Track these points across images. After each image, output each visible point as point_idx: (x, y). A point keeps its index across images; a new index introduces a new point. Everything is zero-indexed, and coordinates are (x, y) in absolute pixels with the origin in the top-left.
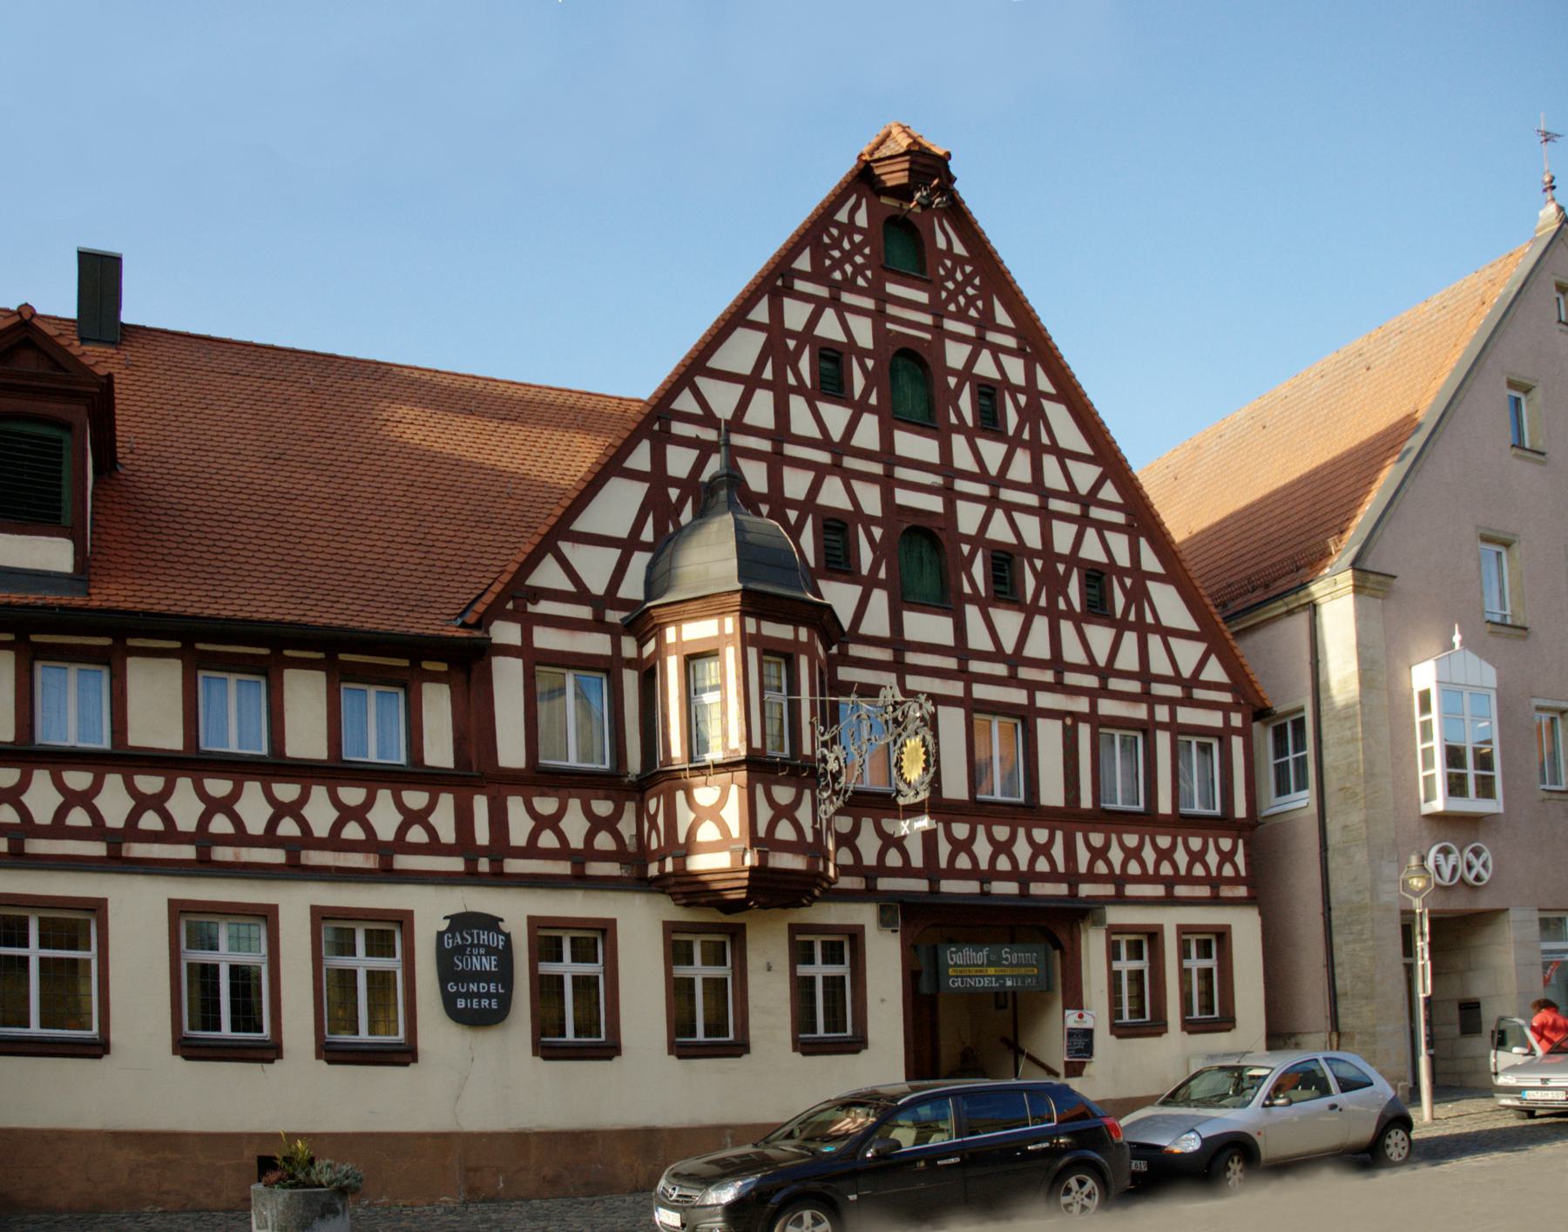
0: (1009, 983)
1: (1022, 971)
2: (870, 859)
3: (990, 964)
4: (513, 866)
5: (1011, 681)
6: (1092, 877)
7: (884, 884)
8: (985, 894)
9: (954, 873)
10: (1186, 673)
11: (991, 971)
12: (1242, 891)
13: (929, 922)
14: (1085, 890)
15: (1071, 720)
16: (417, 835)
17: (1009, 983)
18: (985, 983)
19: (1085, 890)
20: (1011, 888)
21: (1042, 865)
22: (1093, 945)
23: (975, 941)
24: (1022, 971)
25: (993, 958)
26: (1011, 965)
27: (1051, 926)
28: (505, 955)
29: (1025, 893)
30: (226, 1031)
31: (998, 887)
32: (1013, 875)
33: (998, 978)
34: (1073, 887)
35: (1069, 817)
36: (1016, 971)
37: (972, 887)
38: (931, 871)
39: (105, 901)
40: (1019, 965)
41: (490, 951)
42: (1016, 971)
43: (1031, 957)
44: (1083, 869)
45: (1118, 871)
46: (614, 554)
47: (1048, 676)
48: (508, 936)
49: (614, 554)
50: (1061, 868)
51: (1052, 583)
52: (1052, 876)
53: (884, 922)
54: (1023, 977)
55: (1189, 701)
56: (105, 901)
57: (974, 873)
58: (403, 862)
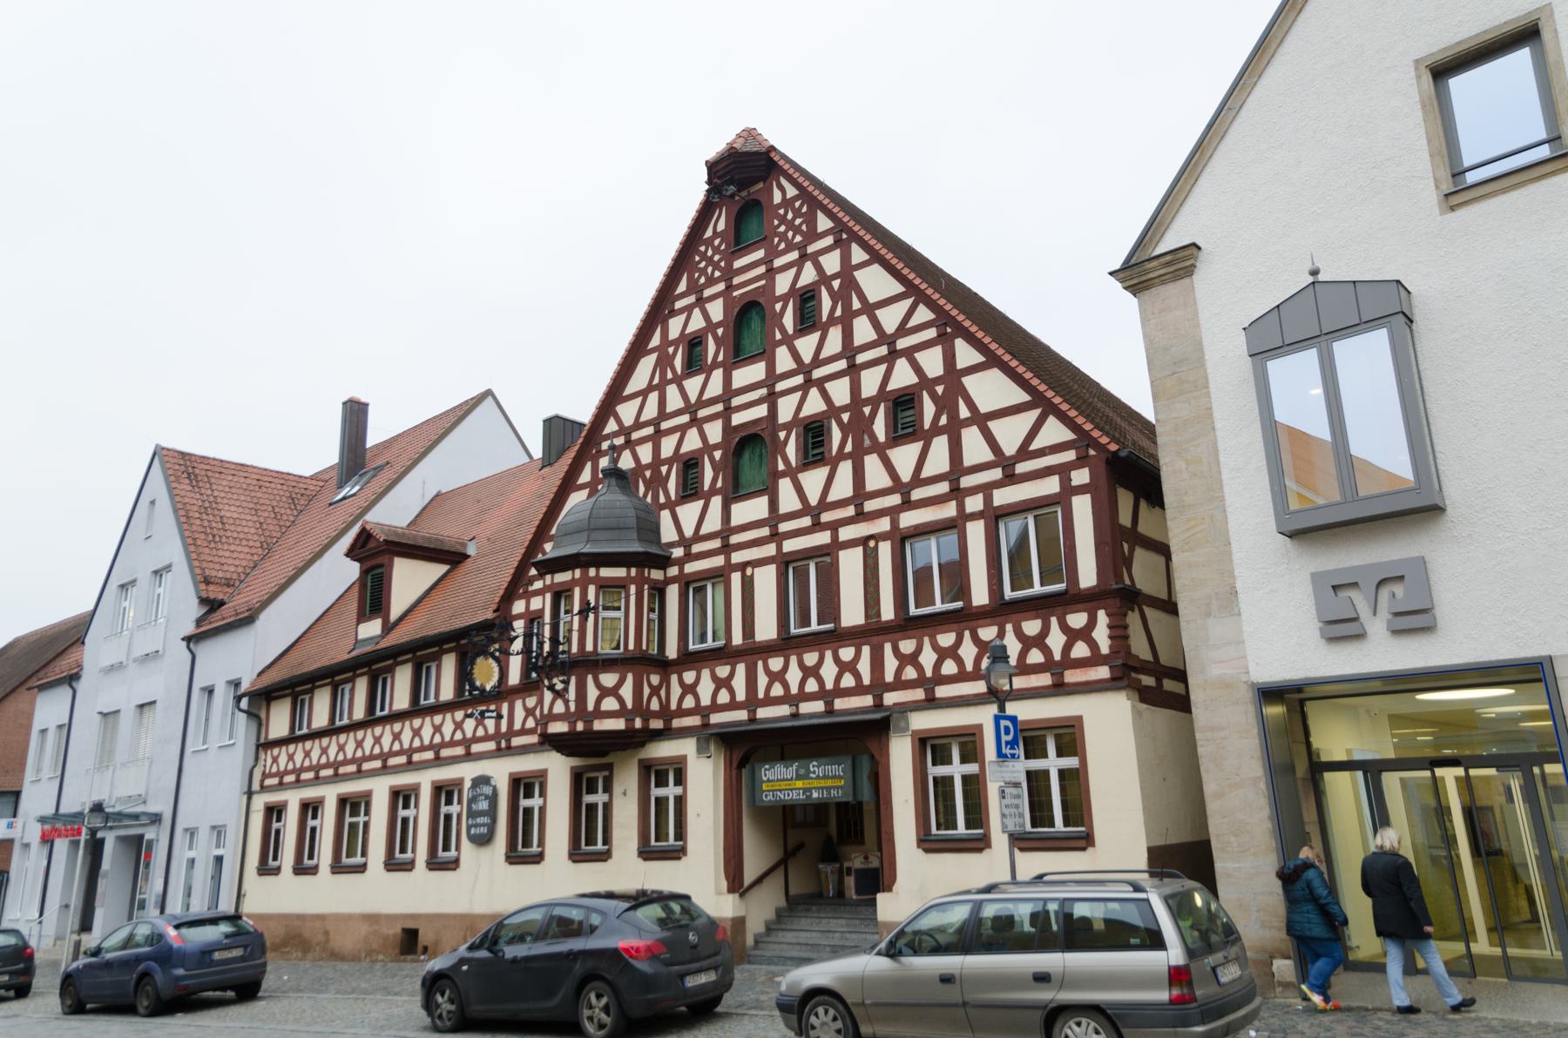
0: (815, 795)
1: (829, 783)
2: (706, 701)
3: (799, 777)
4: (516, 741)
5: (817, 526)
6: (899, 684)
7: (715, 718)
8: (795, 716)
9: (769, 701)
10: (814, 500)
11: (799, 784)
12: (1103, 672)
13: (746, 748)
14: (890, 698)
15: (867, 544)
16: (949, 668)
17: (815, 795)
18: (794, 796)
19: (890, 698)
20: (818, 706)
21: (848, 681)
22: (901, 755)
23: (784, 757)
24: (829, 783)
25: (802, 772)
26: (818, 777)
27: (860, 739)
28: (493, 799)
29: (830, 711)
30: (962, 829)
31: (806, 708)
32: (822, 694)
33: (805, 790)
34: (753, 712)
35: (873, 632)
36: (823, 783)
37: (784, 710)
38: (752, 702)
39: (1079, 719)
40: (825, 777)
41: (487, 797)
42: (823, 783)
43: (836, 769)
44: (889, 677)
45: (1057, 657)
46: (993, 425)
47: (895, 500)
48: (495, 788)
49: (993, 425)
50: (866, 681)
51: (859, 427)
52: (859, 690)
53: (701, 750)
54: (829, 789)
55: (908, 504)
56: (1079, 719)
57: (787, 699)
58: (942, 692)
